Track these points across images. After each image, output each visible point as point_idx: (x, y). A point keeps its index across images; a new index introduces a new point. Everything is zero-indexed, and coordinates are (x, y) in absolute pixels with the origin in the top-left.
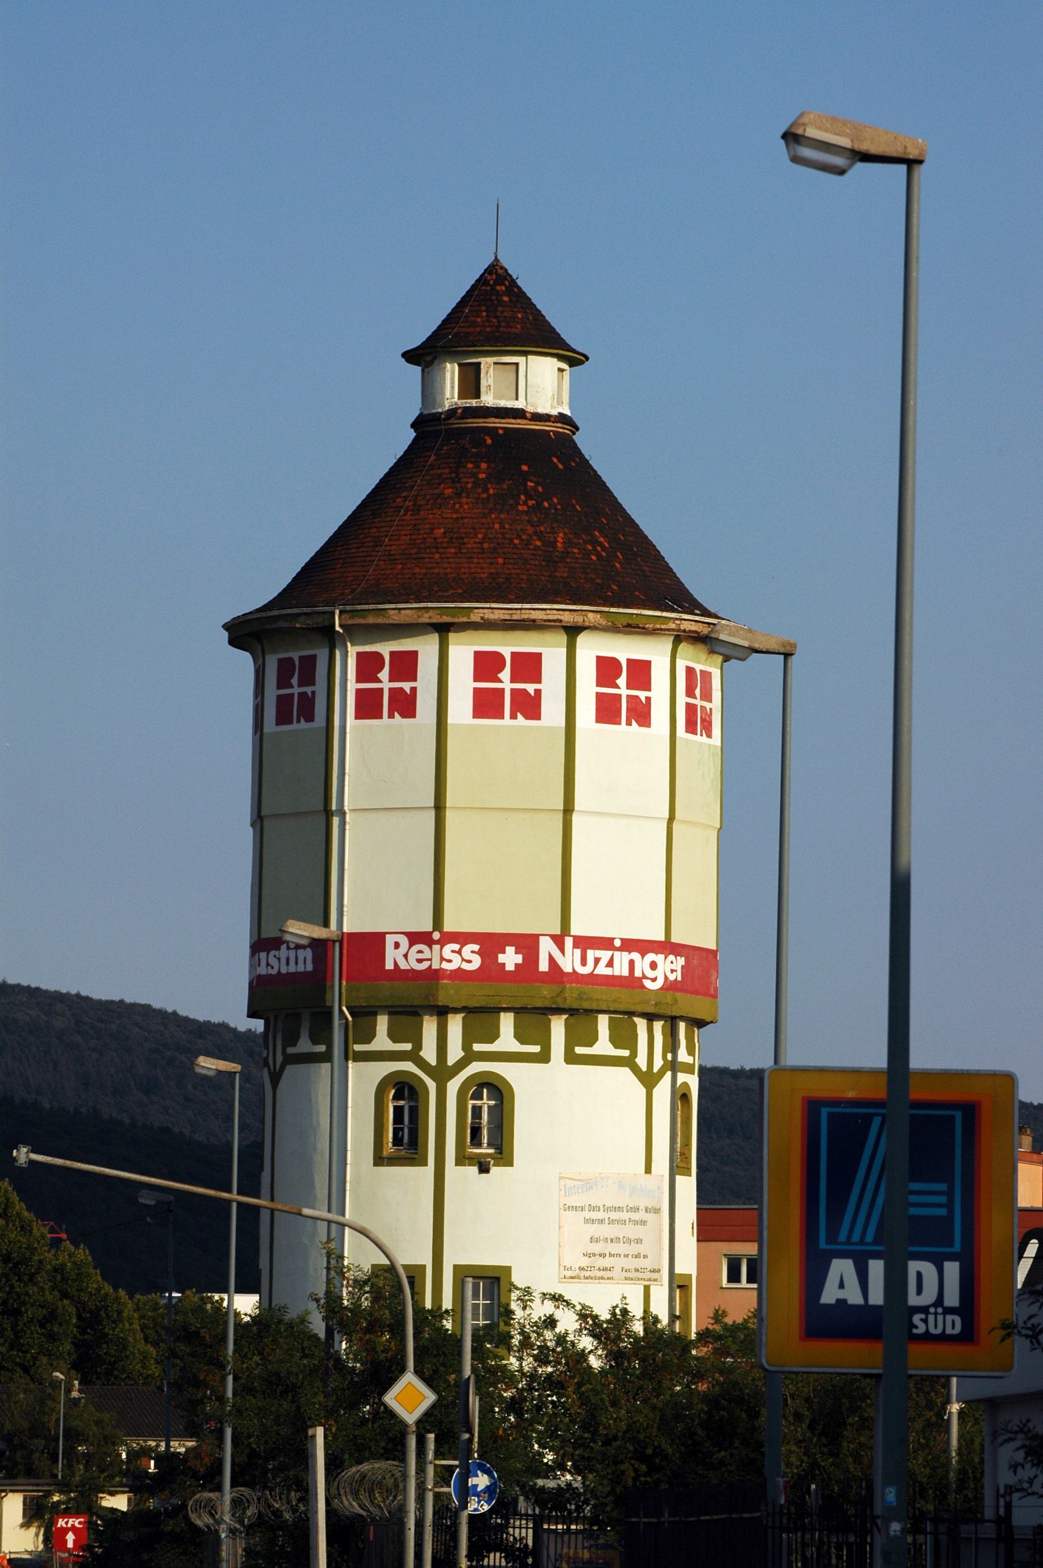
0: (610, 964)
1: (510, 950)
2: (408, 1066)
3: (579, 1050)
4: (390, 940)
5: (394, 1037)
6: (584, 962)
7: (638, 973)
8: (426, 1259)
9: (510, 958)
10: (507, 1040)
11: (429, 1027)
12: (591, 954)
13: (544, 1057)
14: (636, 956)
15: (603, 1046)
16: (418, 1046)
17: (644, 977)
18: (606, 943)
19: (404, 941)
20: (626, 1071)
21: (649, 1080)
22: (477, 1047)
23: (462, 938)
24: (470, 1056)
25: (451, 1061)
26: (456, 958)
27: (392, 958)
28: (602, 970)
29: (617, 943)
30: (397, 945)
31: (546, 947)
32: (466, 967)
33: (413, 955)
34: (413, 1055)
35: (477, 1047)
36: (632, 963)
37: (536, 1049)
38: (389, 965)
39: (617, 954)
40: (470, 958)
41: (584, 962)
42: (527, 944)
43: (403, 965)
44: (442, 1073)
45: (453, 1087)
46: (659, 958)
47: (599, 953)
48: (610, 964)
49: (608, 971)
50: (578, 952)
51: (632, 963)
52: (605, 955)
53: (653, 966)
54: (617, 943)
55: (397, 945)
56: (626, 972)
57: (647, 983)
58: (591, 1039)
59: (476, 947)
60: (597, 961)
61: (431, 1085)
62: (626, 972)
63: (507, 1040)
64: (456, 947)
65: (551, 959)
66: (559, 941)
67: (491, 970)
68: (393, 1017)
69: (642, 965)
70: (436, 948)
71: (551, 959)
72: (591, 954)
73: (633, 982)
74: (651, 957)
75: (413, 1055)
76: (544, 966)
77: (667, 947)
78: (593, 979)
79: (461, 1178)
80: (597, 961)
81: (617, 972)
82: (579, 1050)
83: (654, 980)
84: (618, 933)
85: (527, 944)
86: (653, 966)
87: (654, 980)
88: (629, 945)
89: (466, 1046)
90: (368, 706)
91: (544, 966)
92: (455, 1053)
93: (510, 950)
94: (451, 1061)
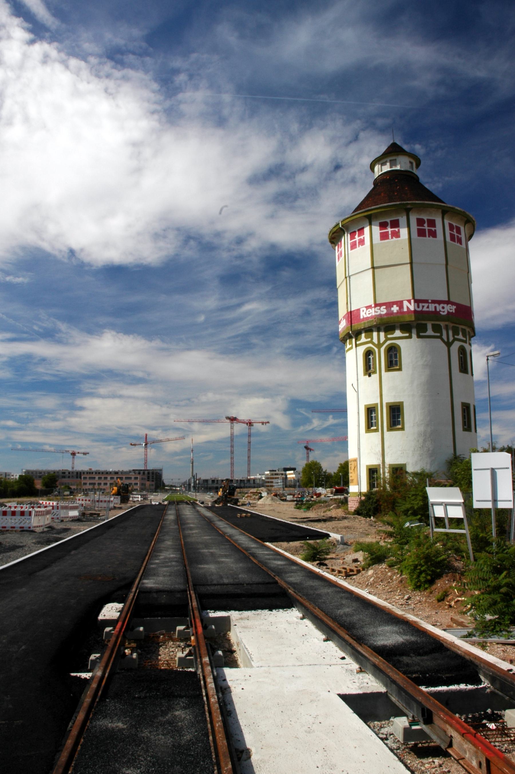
0: (428, 307)
1: (395, 306)
2: (370, 345)
3: (421, 334)
4: (361, 310)
5: (366, 337)
6: (418, 307)
7: (438, 310)
8: (378, 401)
9: (395, 309)
10: (398, 333)
11: (375, 334)
12: (421, 305)
13: (410, 337)
14: (437, 305)
15: (430, 332)
16: (372, 339)
17: (440, 311)
18: (426, 301)
19: (365, 309)
20: (439, 340)
21: (449, 344)
22: (389, 336)
23: (380, 305)
24: (387, 339)
25: (381, 342)
26: (379, 311)
27: (363, 314)
28: (425, 309)
29: (430, 301)
30: (363, 311)
31: (406, 304)
32: (382, 313)
33: (367, 313)
34: (371, 342)
35: (389, 336)
36: (435, 307)
37: (407, 335)
38: (362, 317)
39: (430, 305)
40: (383, 311)
41: (418, 307)
42: (400, 304)
43: (365, 316)
44: (379, 346)
45: (383, 349)
46: (445, 306)
47: (423, 304)
48: (428, 307)
49: (428, 310)
50: (416, 304)
51: (435, 307)
52: (426, 305)
53: (443, 308)
54: (430, 301)
55: (363, 311)
56: (433, 310)
57: (442, 313)
58: (425, 330)
59: (385, 307)
60: (423, 307)
61: (376, 350)
62: (433, 310)
63: (398, 333)
64: (379, 308)
65: (408, 308)
66: (409, 301)
67: (390, 313)
68: (367, 334)
69: (439, 308)
70: (373, 309)
71: (408, 308)
72: (421, 305)
73: (436, 313)
74: (442, 305)
75: (371, 342)
76: (405, 309)
77: (448, 302)
78: (422, 312)
80: (423, 307)
81: (430, 310)
82: (421, 334)
83: (444, 312)
84: (430, 299)
85: (400, 304)
86: (443, 308)
87: (444, 312)
88: (434, 302)
89: (386, 336)
90: (353, 246)
91: (405, 309)
92: (382, 339)
93: (395, 306)
94: (381, 342)
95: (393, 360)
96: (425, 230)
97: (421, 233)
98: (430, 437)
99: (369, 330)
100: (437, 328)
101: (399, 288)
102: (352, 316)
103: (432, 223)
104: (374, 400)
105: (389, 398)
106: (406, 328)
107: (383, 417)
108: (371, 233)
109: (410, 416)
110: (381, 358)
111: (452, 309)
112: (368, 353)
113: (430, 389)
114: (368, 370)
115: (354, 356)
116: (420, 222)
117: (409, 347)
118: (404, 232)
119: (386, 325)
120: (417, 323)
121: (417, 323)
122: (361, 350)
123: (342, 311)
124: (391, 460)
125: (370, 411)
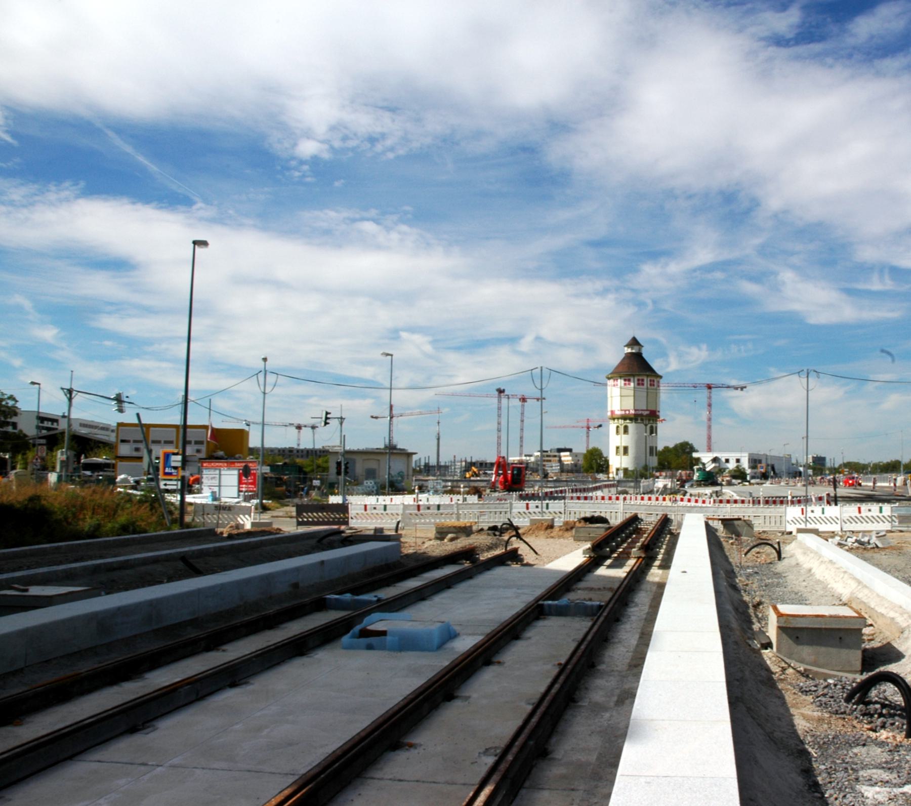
21: (646, 425)
79: (624, 436)
95: (626, 430)
96: (640, 383)
97: (638, 384)
98: (637, 459)
99: (618, 419)
100: (642, 420)
101: (629, 406)
102: (612, 412)
103: (643, 380)
104: (619, 445)
105: (624, 444)
106: (631, 419)
107: (622, 450)
108: (620, 382)
109: (630, 451)
110: (622, 430)
111: (648, 412)
112: (618, 427)
113: (637, 443)
114: (617, 432)
115: (613, 426)
116: (638, 380)
117: (632, 426)
118: (632, 384)
119: (624, 418)
120: (635, 418)
121: (635, 418)
122: (615, 426)
123: (609, 409)
124: (624, 466)
125: (618, 448)
